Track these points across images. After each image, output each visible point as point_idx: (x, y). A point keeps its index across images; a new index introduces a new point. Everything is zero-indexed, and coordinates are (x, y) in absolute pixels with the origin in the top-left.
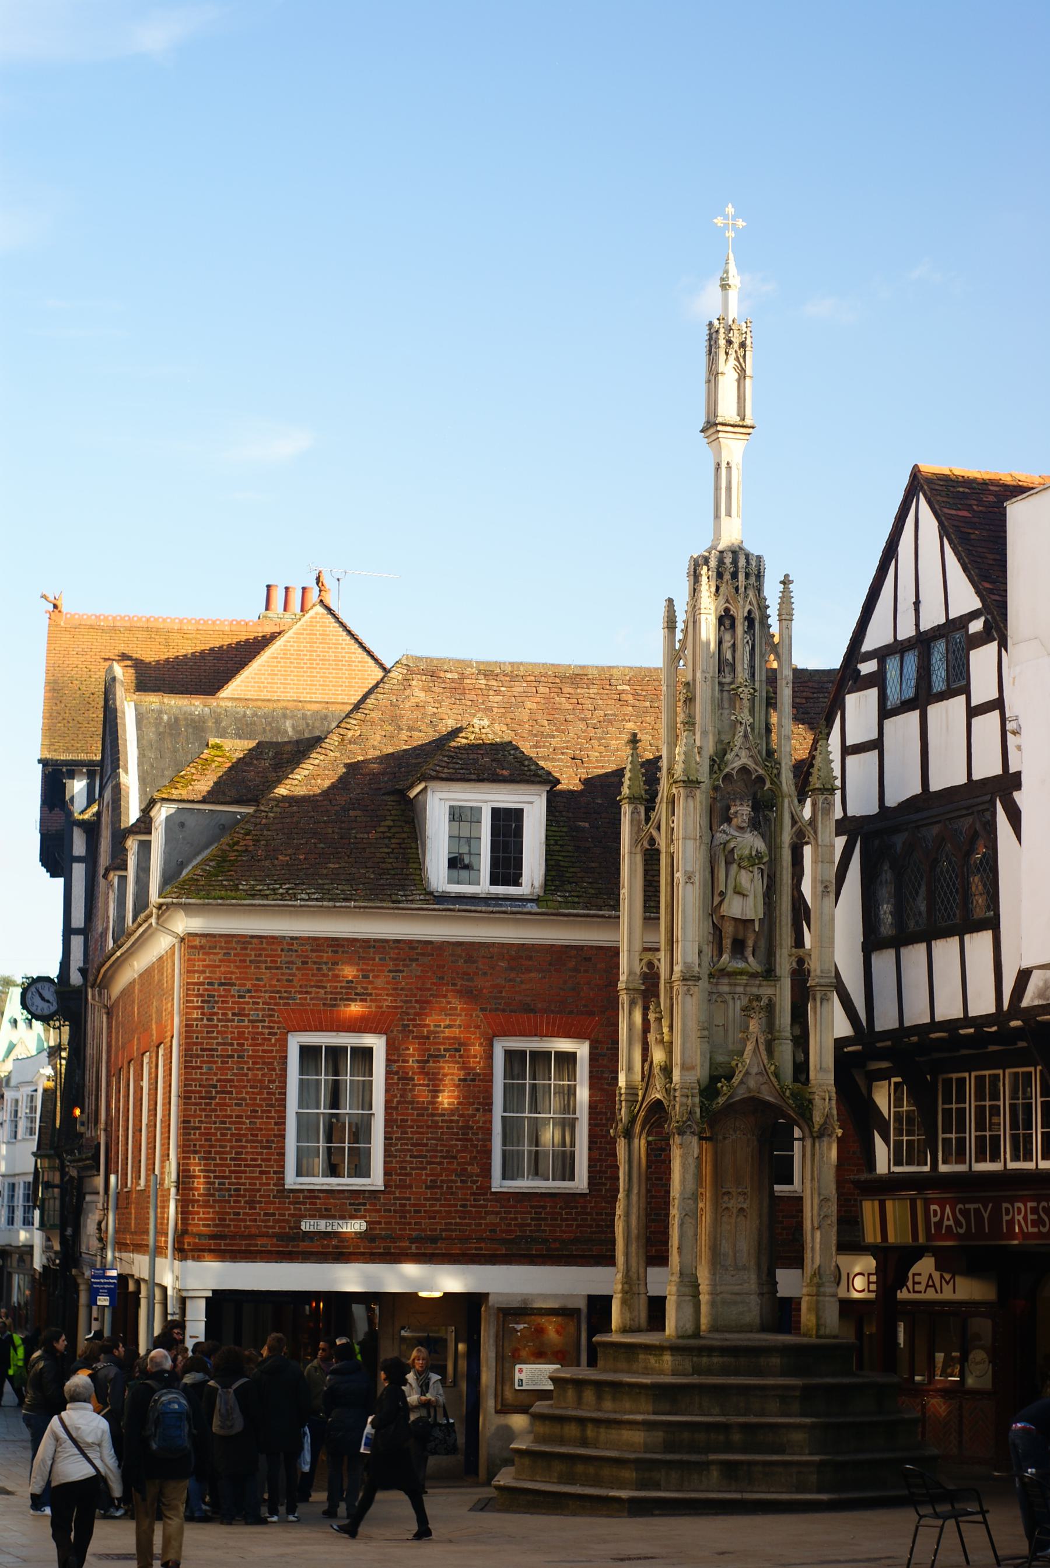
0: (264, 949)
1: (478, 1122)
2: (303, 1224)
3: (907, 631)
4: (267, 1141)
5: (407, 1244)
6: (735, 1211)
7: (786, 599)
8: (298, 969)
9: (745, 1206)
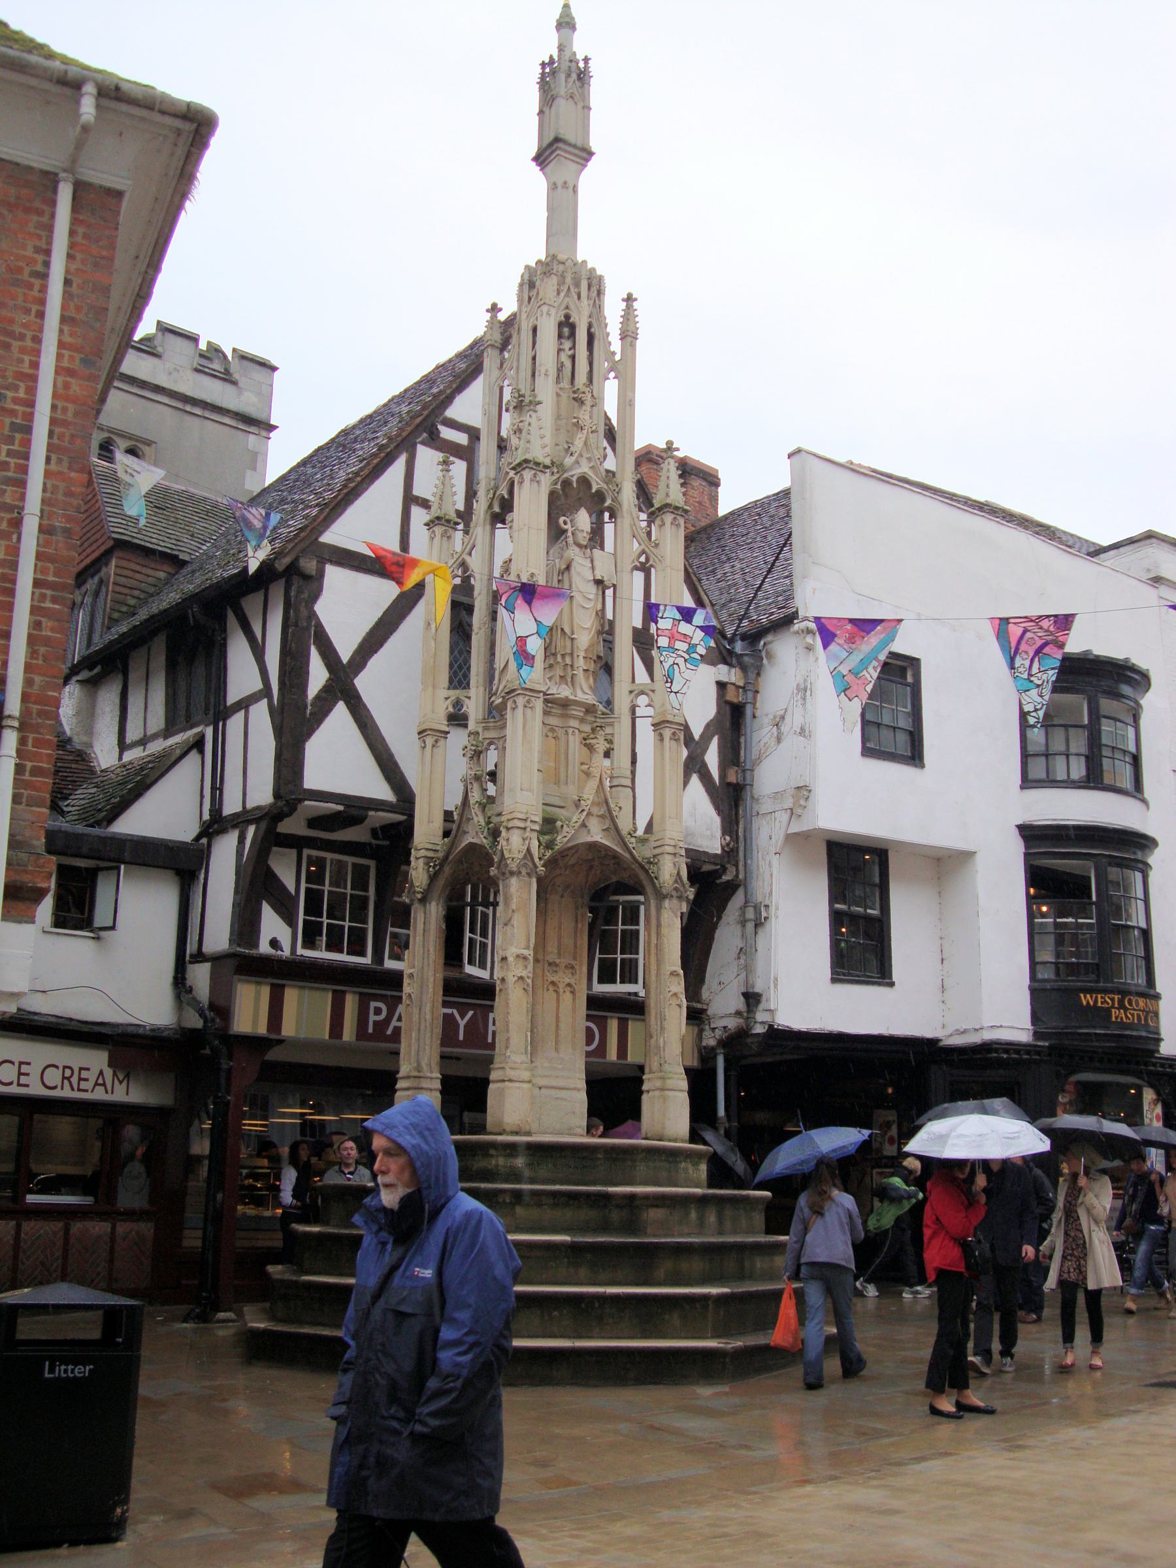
7: (629, 316)
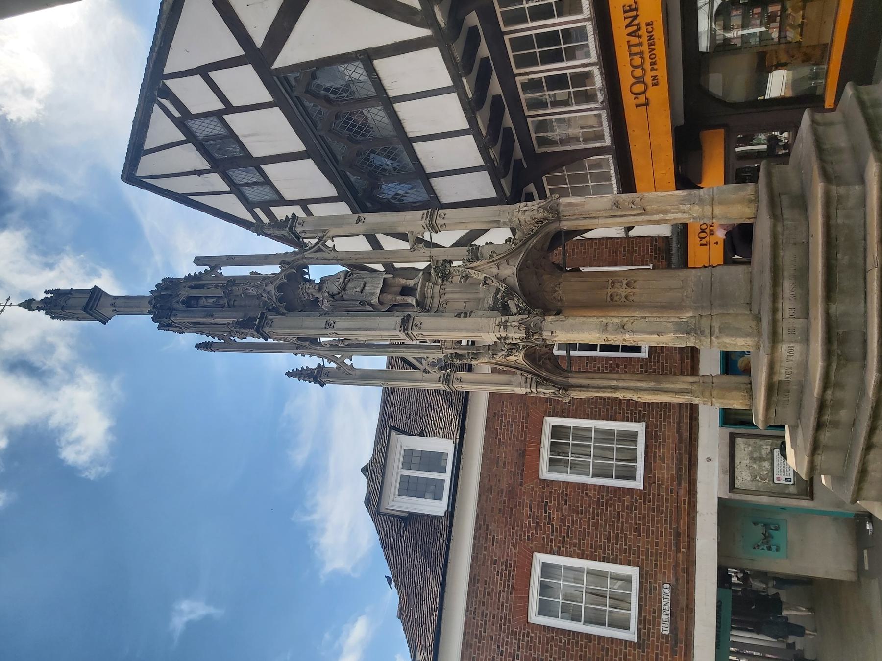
0: (473, 631)
1: (594, 494)
2: (664, 632)
3: (216, 181)
4: (603, 650)
5: (680, 555)
6: (629, 290)
8: (487, 609)
9: (625, 282)
